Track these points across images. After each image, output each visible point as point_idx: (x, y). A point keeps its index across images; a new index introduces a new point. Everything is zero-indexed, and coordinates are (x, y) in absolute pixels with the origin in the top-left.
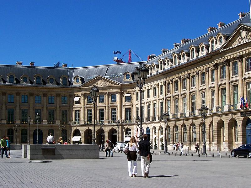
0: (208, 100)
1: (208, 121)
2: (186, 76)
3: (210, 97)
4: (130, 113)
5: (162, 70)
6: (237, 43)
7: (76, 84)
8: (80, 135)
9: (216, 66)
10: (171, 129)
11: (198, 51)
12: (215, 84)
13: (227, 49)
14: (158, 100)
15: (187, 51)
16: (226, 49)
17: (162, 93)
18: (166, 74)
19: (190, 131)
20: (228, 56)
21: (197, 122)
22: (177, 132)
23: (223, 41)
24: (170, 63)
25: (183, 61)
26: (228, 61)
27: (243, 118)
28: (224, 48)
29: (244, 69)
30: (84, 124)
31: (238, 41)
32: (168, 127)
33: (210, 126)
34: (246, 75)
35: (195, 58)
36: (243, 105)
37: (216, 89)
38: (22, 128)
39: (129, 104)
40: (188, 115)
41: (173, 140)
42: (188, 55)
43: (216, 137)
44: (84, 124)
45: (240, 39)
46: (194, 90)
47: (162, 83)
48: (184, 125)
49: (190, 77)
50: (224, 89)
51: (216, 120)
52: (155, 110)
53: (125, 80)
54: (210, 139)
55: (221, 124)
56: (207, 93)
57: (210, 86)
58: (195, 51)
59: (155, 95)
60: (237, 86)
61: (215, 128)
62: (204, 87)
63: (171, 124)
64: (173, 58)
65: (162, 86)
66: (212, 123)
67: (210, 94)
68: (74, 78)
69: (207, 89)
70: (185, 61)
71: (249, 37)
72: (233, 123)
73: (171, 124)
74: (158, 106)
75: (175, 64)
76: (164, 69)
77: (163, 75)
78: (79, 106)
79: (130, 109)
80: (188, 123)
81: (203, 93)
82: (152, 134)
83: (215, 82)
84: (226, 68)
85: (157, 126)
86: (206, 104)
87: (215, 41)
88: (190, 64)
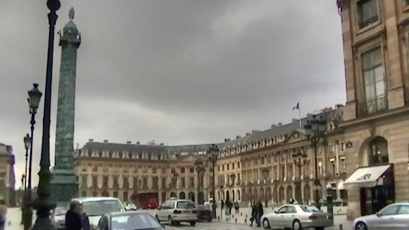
10: (247, 192)
12: (277, 164)
17: (239, 167)
18: (242, 154)
25: (255, 147)
36: (295, 178)
40: (259, 182)
55: (282, 188)
57: (274, 164)
65: (239, 163)
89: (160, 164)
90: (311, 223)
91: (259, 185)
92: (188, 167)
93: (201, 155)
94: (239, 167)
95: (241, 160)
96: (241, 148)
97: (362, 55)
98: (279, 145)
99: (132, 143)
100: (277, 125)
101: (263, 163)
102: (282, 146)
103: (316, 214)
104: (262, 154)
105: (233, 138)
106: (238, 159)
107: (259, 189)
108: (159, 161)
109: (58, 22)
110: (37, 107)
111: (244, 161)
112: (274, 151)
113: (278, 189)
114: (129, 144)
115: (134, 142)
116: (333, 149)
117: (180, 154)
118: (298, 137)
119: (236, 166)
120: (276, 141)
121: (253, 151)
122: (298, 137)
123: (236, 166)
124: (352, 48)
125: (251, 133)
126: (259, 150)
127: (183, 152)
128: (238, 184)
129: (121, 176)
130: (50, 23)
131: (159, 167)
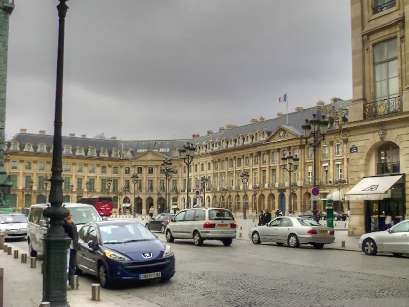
8: (129, 202)
9: (259, 153)
10: (218, 199)
17: (209, 169)
20: (269, 147)
25: (229, 146)
27: (279, 193)
35: (241, 144)
36: (279, 185)
38: (25, 193)
42: (235, 141)
55: (262, 196)
57: (253, 168)
59: (203, 170)
62: (249, 168)
63: (219, 195)
69: (251, 170)
71: (285, 136)
89: (110, 163)
90: (310, 238)
91: (233, 191)
92: (146, 166)
93: (161, 153)
94: (209, 169)
95: (212, 161)
96: (213, 145)
97: (374, 45)
98: (260, 144)
99: (76, 136)
100: (258, 120)
101: (239, 165)
103: (315, 228)
104: (238, 154)
105: (203, 133)
106: (209, 159)
107: (233, 195)
108: (111, 159)
109: (68, 14)
110: (297, 166)
112: (254, 151)
113: (257, 196)
116: (327, 152)
117: (136, 151)
118: (284, 136)
119: (206, 166)
120: (256, 140)
122: (284, 136)
123: (206, 166)
124: (363, 36)
125: (226, 128)
126: (234, 150)
127: (140, 149)
130: (60, 15)
131: (110, 166)
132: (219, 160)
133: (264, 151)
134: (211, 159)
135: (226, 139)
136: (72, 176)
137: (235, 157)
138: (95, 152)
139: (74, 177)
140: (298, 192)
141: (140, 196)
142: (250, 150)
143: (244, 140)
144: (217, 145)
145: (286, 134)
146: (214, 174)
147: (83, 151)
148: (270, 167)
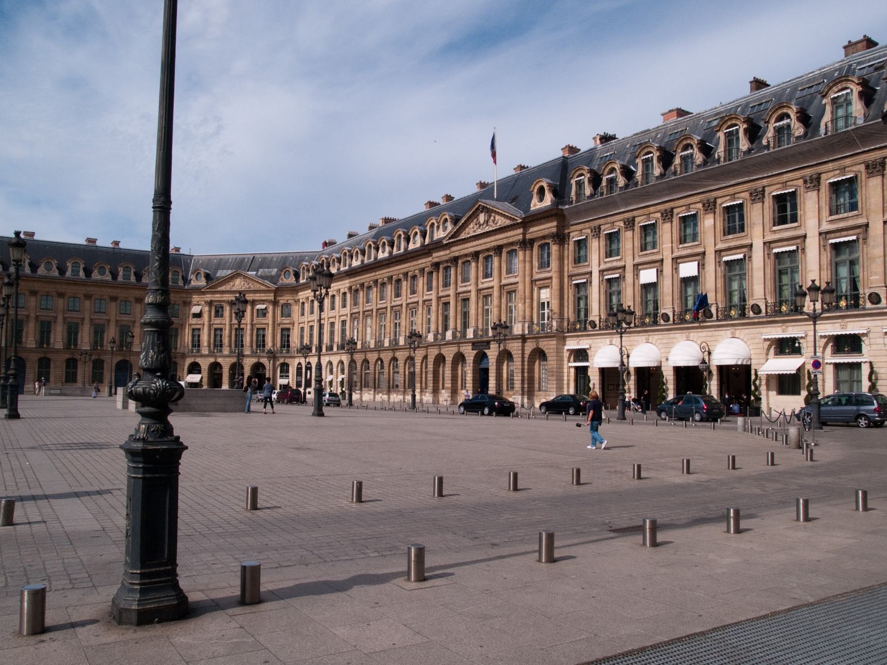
0: (420, 321)
1: (419, 355)
2: (386, 279)
3: (424, 316)
4: (288, 336)
5: (347, 268)
6: (472, 230)
7: (196, 284)
8: (200, 372)
9: (436, 265)
11: (408, 240)
12: (433, 295)
13: (455, 239)
14: (337, 317)
15: (389, 238)
16: (452, 240)
17: (344, 306)
18: (352, 273)
19: (389, 369)
20: (456, 251)
21: (401, 355)
22: (368, 371)
23: (450, 227)
24: (359, 256)
25: (382, 255)
26: (455, 260)
27: (475, 352)
28: (450, 238)
29: (481, 274)
30: (207, 353)
31: (473, 228)
32: (352, 362)
33: (422, 363)
34: (483, 283)
35: (402, 250)
36: (475, 332)
37: (434, 303)
38: (94, 357)
39: (288, 322)
40: (387, 344)
41: (361, 385)
42: (392, 244)
43: (432, 382)
44: (207, 353)
45: (476, 224)
46: (399, 303)
47: (346, 289)
48: (380, 359)
49: (393, 282)
50: (447, 304)
51: (433, 353)
52: (332, 333)
53: (282, 279)
54: (421, 383)
55: (440, 359)
56: (420, 309)
57: (425, 298)
58: (402, 239)
59: (333, 308)
60: (468, 299)
61: (431, 367)
62: (415, 300)
63: (359, 358)
64: (366, 248)
65: (345, 294)
66: (425, 357)
67: (425, 312)
68: (193, 273)
69: (421, 303)
70: (386, 255)
71: (491, 223)
72: (460, 358)
73: (359, 358)
74: (338, 327)
75: (369, 258)
76: (350, 265)
77: (348, 275)
78: (199, 322)
79: (288, 329)
80: (386, 357)
81: (412, 308)
82: (326, 373)
83: (433, 292)
84: (496, 260)
85: (335, 360)
86: (418, 328)
87: (436, 225)
88: (394, 260)
93: (262, 277)
94: (344, 306)
95: (350, 288)
96: (351, 257)
98: (438, 246)
99: (98, 243)
100: (442, 202)
102: (448, 246)
104: (396, 270)
105: (341, 238)
111: (357, 291)
112: (425, 262)
113: (431, 360)
114: (91, 244)
115: (104, 242)
117: (216, 273)
121: (379, 265)
128: (342, 347)
129: (60, 319)
132: (362, 285)
133: (447, 261)
134: (348, 285)
135: (374, 243)
136: (83, 319)
137: (392, 276)
138: (132, 273)
139: (87, 321)
140: (514, 347)
141: (219, 360)
142: (420, 262)
143: (408, 242)
144: (359, 255)
145: (492, 218)
146: (352, 314)
147: (107, 272)
148: (457, 294)
